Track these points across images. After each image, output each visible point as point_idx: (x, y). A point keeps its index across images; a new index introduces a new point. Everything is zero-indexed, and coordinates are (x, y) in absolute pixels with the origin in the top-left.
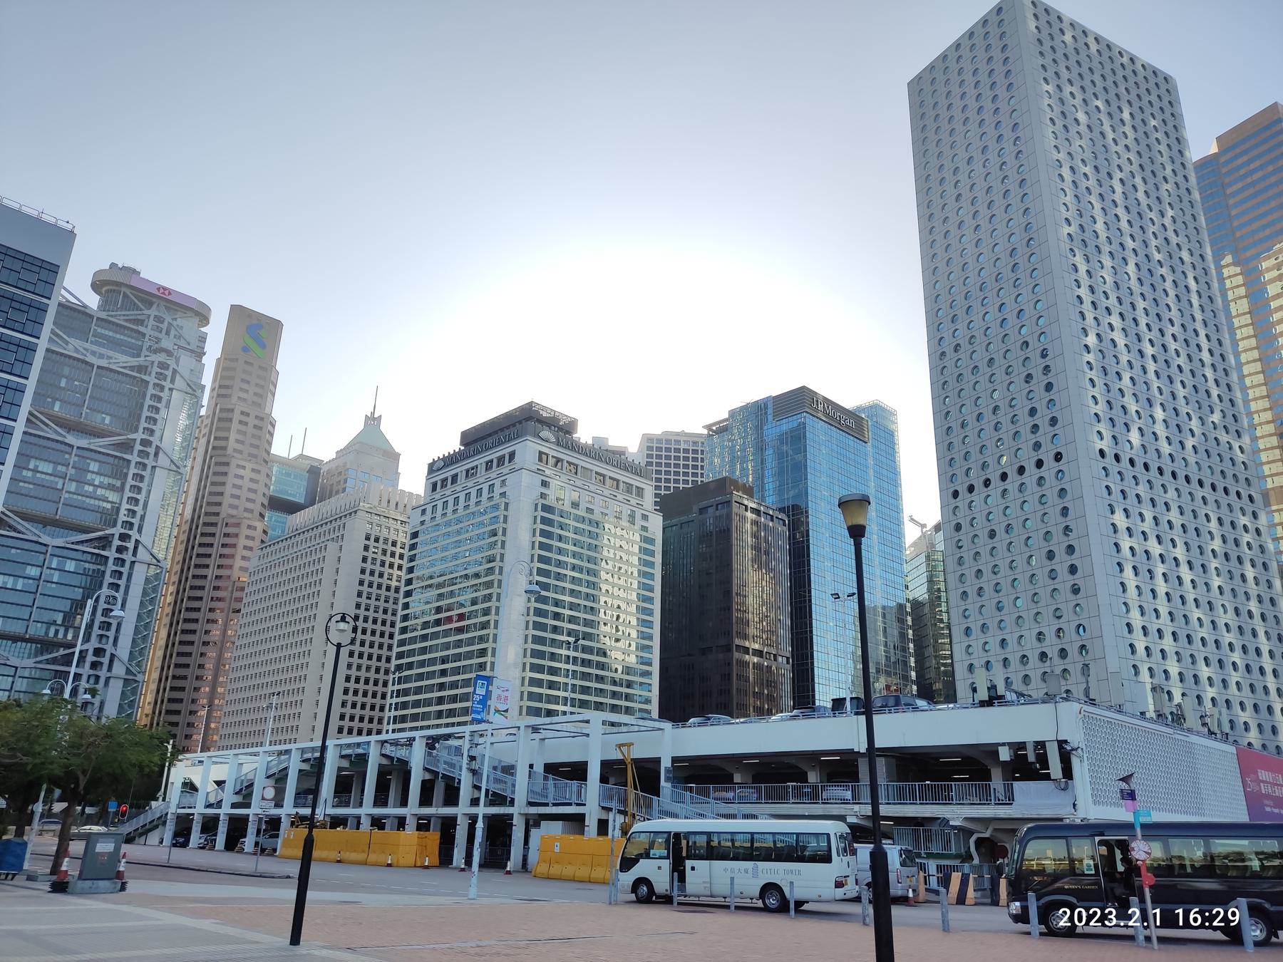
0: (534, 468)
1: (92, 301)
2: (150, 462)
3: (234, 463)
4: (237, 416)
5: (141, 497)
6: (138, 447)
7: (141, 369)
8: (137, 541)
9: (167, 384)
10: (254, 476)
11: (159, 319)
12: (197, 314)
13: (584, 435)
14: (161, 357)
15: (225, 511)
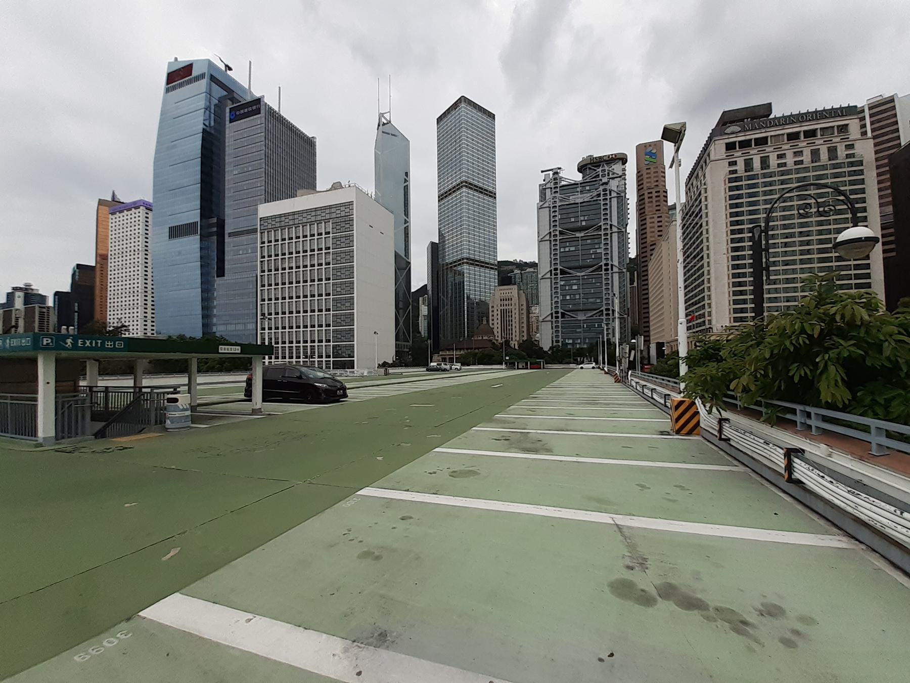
0: (724, 157)
1: (579, 177)
2: (609, 232)
3: (648, 217)
4: (646, 196)
5: (609, 247)
6: (603, 227)
7: (599, 195)
8: (612, 265)
9: (608, 197)
10: (659, 219)
11: (604, 171)
12: (619, 159)
13: (776, 113)
14: (601, 188)
15: (649, 240)
